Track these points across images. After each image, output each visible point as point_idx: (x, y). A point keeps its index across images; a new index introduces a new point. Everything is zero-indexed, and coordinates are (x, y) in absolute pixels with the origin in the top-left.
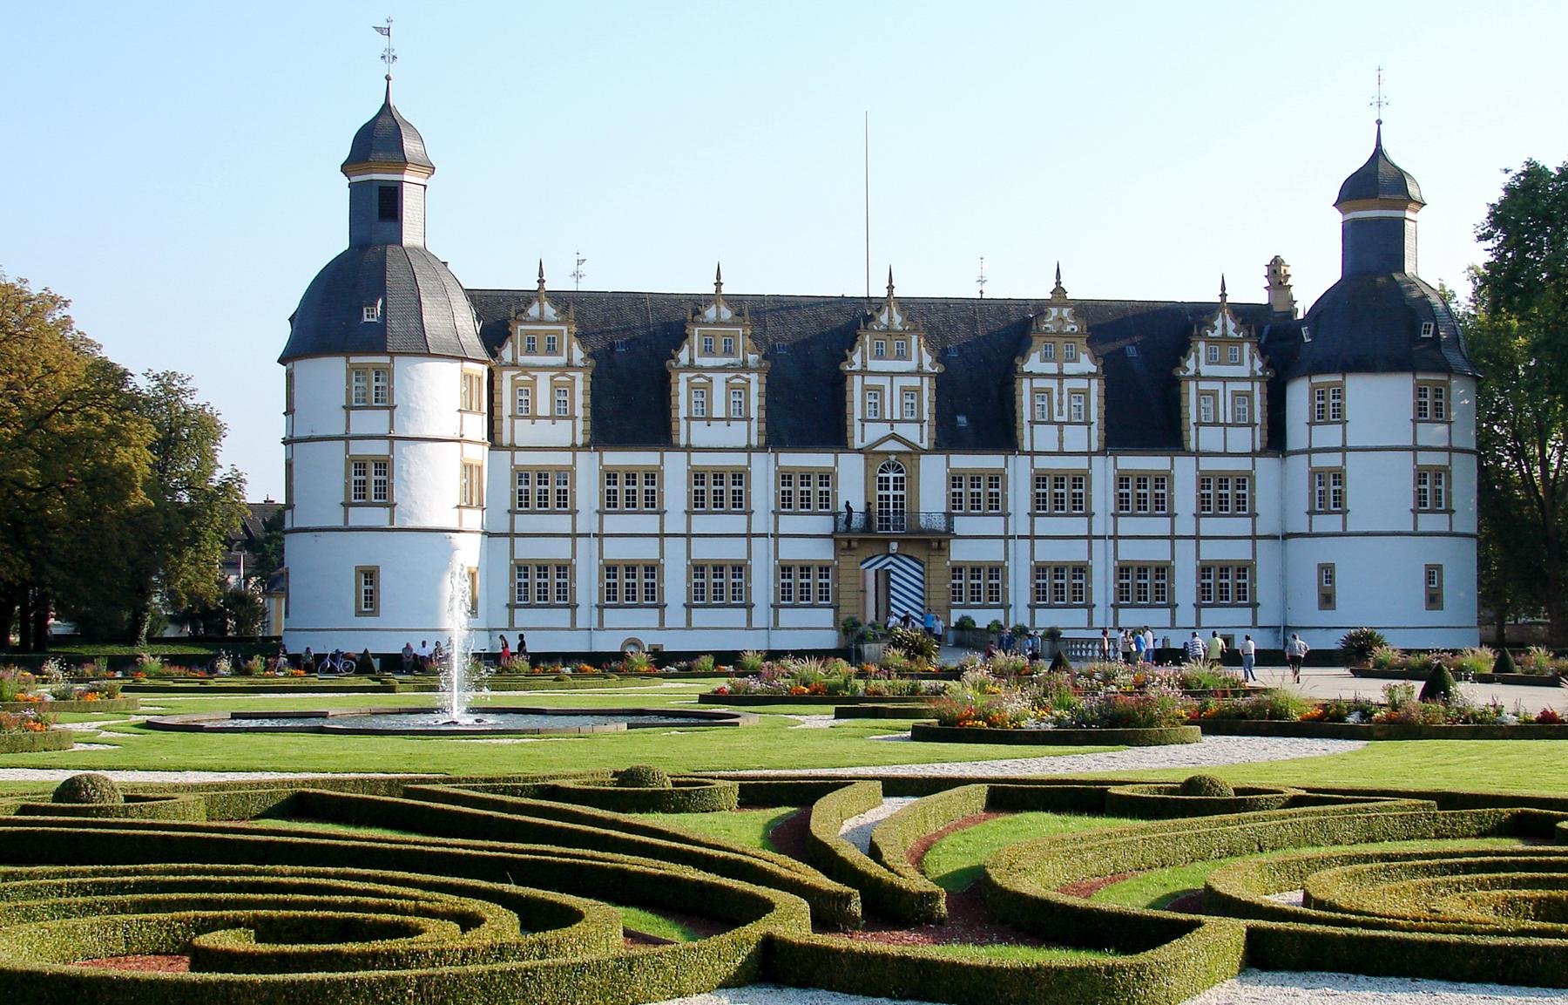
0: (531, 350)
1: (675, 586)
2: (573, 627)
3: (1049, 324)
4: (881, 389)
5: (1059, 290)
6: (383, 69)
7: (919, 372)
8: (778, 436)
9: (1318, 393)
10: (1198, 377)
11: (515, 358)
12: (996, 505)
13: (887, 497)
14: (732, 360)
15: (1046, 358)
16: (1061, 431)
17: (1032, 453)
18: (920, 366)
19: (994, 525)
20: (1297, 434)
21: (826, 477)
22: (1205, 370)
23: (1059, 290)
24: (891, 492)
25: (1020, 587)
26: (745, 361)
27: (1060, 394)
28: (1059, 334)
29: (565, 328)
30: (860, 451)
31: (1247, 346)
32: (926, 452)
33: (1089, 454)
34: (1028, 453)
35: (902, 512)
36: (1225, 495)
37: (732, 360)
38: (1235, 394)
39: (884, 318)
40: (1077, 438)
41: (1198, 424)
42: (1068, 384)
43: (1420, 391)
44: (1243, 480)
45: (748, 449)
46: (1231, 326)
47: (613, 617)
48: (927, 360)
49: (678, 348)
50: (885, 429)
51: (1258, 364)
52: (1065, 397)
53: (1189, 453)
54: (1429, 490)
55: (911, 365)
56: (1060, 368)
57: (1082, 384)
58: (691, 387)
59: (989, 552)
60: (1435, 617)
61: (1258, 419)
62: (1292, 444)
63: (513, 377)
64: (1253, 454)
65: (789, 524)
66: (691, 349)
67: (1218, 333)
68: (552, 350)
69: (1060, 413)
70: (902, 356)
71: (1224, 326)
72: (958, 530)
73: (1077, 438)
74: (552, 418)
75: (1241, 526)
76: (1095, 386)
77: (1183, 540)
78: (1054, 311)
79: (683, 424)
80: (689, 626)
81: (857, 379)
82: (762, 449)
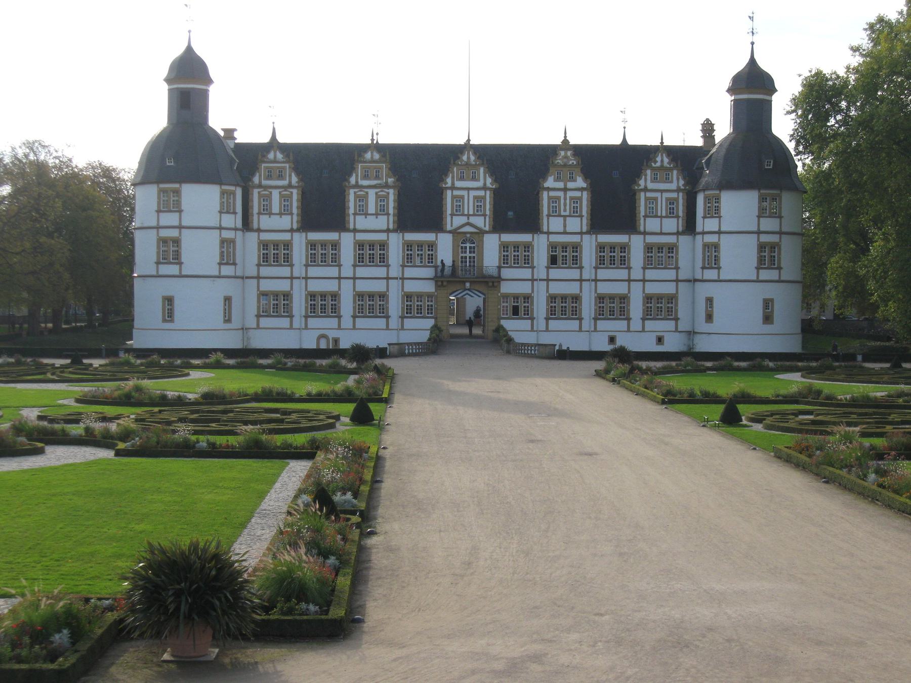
0: (269, 177)
1: (347, 305)
2: (291, 328)
3: (559, 161)
4: (462, 197)
5: (565, 141)
7: (484, 188)
8: (404, 224)
9: (707, 199)
10: (646, 190)
11: (260, 182)
12: (528, 262)
13: (466, 257)
14: (379, 182)
15: (558, 179)
16: (565, 221)
17: (548, 233)
18: (485, 184)
19: (526, 273)
20: (702, 224)
21: (432, 246)
22: (650, 186)
23: (565, 141)
24: (468, 255)
25: (540, 307)
26: (387, 182)
27: (565, 199)
28: (565, 165)
29: (287, 165)
30: (450, 232)
31: (675, 172)
32: (487, 232)
33: (581, 233)
34: (545, 233)
35: (474, 266)
36: (660, 255)
37: (379, 182)
38: (667, 199)
39: (465, 158)
40: (574, 224)
41: (645, 216)
42: (569, 194)
43: (762, 199)
44: (672, 248)
45: (388, 231)
46: (666, 160)
47: (312, 322)
48: (489, 181)
49: (350, 175)
50: (463, 220)
51: (682, 182)
52: (568, 201)
53: (640, 233)
54: (768, 256)
55: (480, 184)
56: (565, 185)
57: (578, 194)
58: (356, 196)
59: (523, 288)
60: (768, 328)
61: (681, 214)
62: (699, 229)
63: (259, 193)
64: (678, 233)
65: (409, 272)
66: (357, 176)
67: (658, 164)
68: (281, 177)
69: (565, 210)
70: (474, 178)
71: (662, 161)
74: (281, 214)
75: (670, 274)
76: (585, 195)
77: (637, 281)
78: (563, 153)
79: (352, 218)
80: (354, 328)
81: (449, 193)
82: (395, 231)
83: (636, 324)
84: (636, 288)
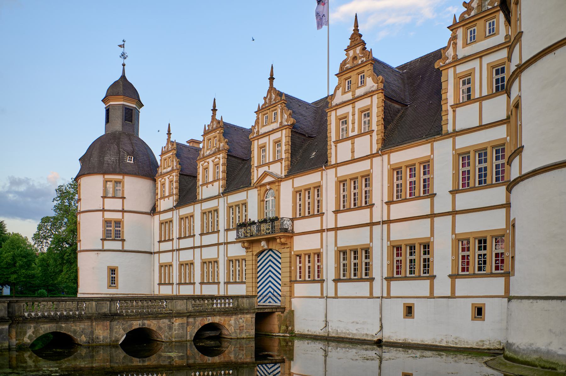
6: (121, 61)
40: (364, 146)
50: (266, 168)
72: (296, 231)
73: (364, 146)
83: (442, 286)
84: (443, 224)
